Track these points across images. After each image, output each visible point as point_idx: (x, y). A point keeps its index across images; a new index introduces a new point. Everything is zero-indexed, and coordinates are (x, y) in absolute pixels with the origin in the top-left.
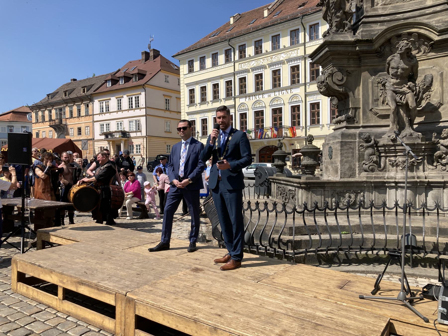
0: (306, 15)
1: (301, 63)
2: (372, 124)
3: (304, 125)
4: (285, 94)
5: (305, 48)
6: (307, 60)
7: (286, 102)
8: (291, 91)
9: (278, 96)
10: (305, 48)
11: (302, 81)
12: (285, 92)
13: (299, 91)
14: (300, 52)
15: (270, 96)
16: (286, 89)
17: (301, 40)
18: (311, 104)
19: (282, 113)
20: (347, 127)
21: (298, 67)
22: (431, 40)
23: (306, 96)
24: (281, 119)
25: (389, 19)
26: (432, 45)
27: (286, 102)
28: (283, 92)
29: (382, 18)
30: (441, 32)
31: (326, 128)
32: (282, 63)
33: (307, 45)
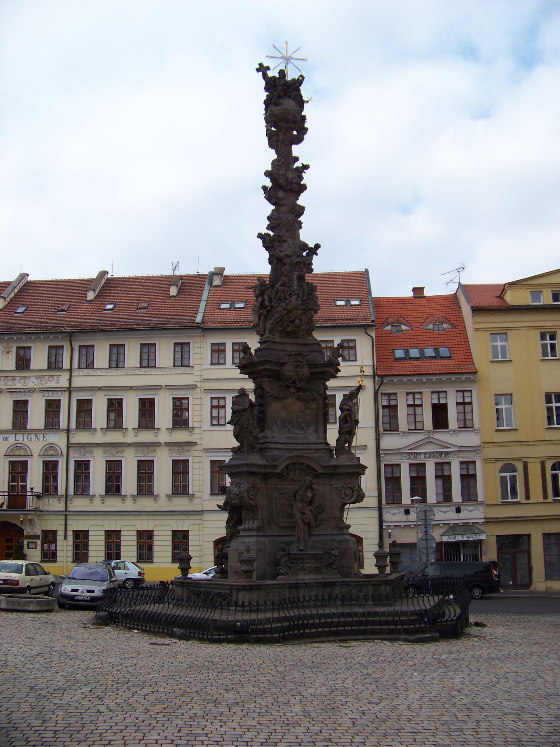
0: (78, 332)
1: (64, 399)
2: (275, 534)
3: (64, 493)
4: (33, 440)
5: (71, 376)
6: (73, 394)
7: (36, 453)
8: (44, 437)
9: (21, 441)
10: (71, 376)
11: (63, 424)
12: (33, 436)
13: (58, 439)
14: (63, 382)
15: (7, 439)
16: (36, 432)
17: (66, 365)
18: (75, 461)
19: (26, 469)
20: (257, 536)
21: (57, 402)
22: (315, 471)
23: (68, 447)
24: (24, 479)
25: (285, 447)
26: (316, 475)
27: (36, 453)
28: (30, 436)
29: (280, 446)
30: (324, 467)
31: (97, 501)
32: (31, 391)
33: (75, 373)
